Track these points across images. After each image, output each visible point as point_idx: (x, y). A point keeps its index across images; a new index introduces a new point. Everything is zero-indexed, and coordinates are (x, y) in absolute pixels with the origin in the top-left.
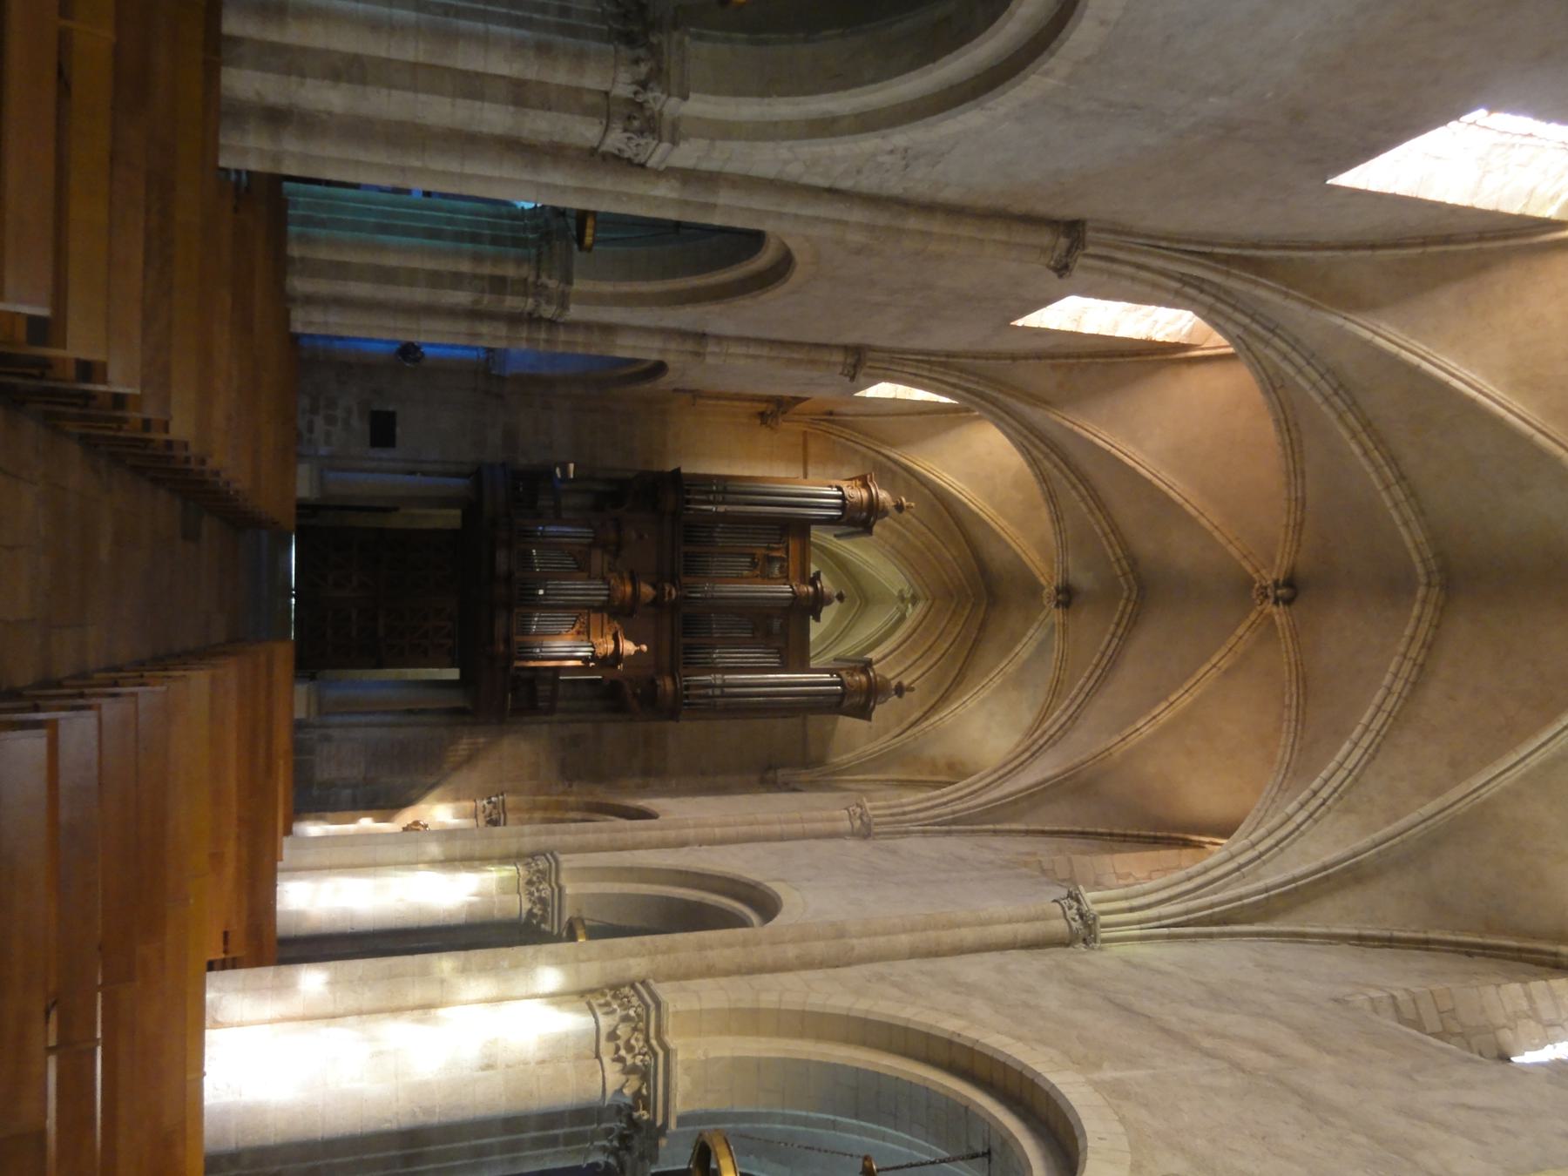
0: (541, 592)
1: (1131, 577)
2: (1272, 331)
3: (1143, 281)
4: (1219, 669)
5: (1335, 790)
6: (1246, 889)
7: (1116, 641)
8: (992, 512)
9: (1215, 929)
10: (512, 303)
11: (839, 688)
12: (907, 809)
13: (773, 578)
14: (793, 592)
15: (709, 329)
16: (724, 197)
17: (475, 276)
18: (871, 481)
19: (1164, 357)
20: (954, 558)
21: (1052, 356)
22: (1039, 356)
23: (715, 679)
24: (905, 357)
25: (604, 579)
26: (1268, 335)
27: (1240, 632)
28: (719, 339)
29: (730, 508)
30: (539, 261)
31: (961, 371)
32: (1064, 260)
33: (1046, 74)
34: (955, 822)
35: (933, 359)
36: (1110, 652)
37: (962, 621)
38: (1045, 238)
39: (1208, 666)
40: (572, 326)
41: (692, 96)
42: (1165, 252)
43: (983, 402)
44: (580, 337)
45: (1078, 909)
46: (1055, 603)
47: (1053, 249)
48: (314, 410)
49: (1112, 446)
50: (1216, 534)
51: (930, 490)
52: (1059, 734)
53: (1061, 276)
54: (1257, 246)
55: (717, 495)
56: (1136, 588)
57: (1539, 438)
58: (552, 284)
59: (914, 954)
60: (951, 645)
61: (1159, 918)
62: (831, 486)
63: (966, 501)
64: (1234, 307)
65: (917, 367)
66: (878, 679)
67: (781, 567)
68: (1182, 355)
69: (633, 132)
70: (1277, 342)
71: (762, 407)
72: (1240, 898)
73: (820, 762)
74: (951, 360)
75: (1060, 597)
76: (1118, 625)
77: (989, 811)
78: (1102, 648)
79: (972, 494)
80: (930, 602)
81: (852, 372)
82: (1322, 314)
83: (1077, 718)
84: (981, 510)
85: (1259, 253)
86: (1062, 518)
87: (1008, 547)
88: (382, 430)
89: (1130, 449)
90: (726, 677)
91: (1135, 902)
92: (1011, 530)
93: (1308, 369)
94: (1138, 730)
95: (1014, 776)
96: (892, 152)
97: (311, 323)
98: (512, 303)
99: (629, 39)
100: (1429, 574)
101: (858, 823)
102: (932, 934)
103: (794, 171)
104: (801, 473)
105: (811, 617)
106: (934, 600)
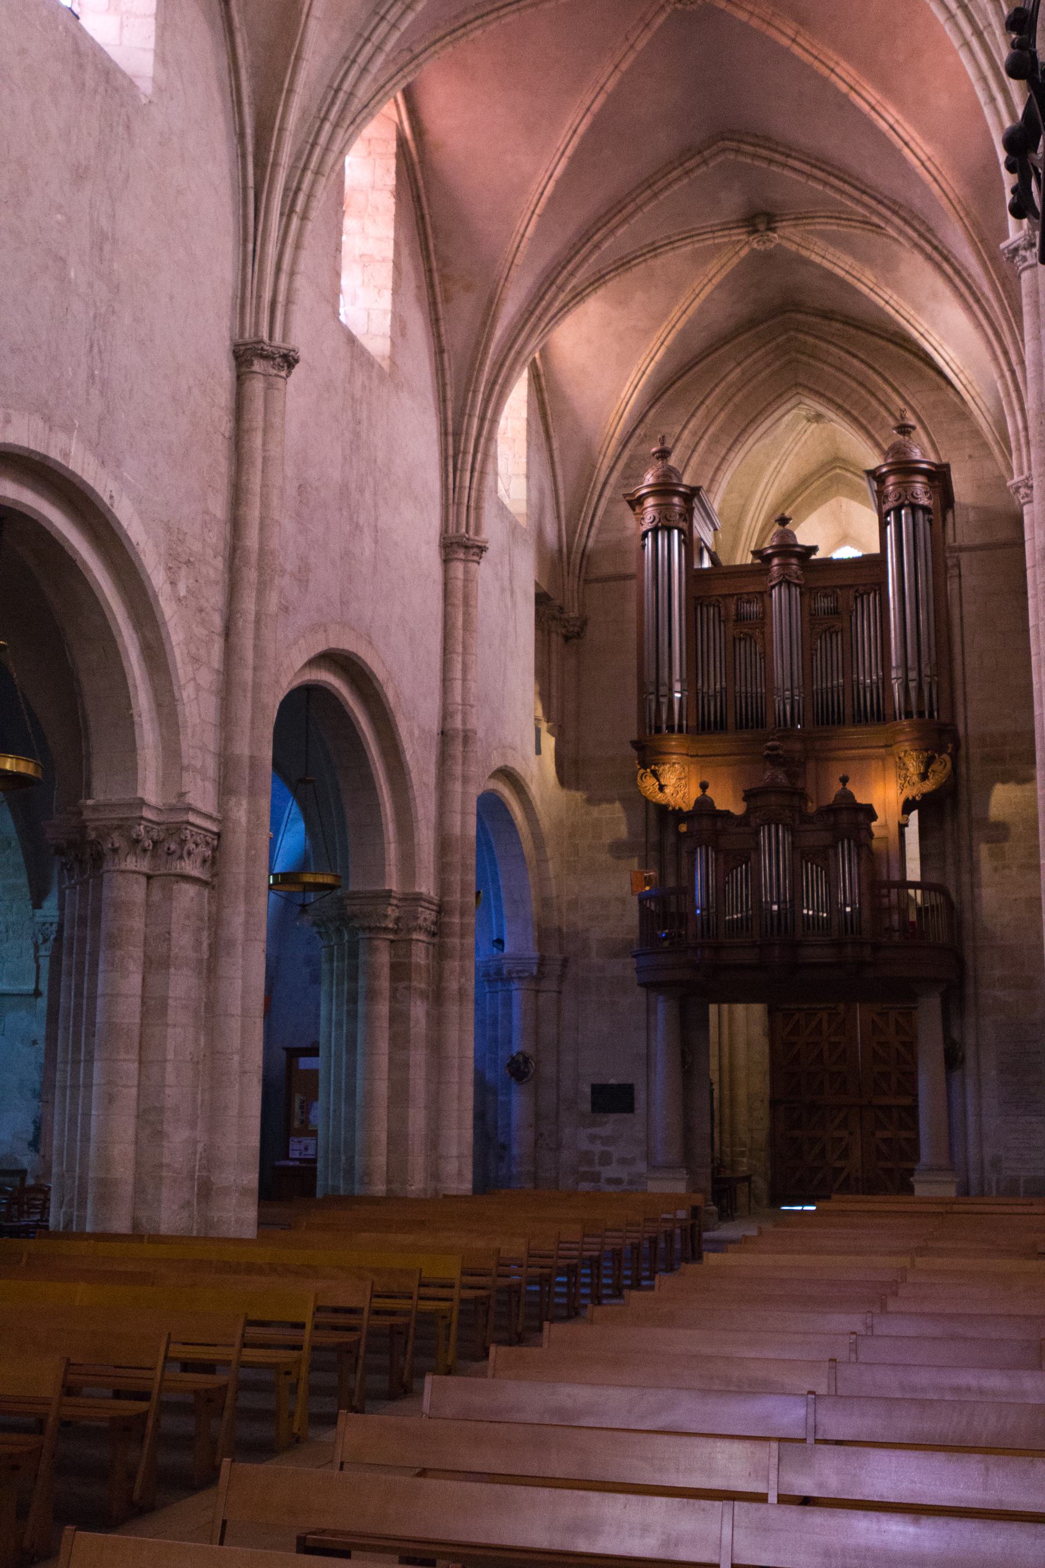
0: (775, 907)
1: (706, 153)
2: (337, 91)
3: (294, 262)
4: (797, 33)
7: (791, 162)
8: (661, 332)
10: (420, 956)
11: (903, 512)
12: (1020, 425)
13: (764, 612)
14: (780, 584)
15: (435, 727)
16: (242, 748)
17: (393, 998)
18: (633, 494)
19: (417, 167)
20: (739, 364)
21: (433, 304)
22: (434, 321)
23: (898, 679)
24: (451, 486)
25: (757, 833)
26: (342, 96)
27: (743, 16)
28: (446, 715)
29: (676, 675)
30: (370, 929)
31: (462, 414)
32: (279, 360)
33: (66, 455)
35: (451, 452)
37: (824, 345)
38: (257, 386)
40: (443, 886)
41: (140, 794)
42: (259, 243)
43: (500, 381)
44: (456, 878)
45: (1025, 249)
46: (771, 234)
48: (595, 1177)
49: (533, 212)
50: (624, 67)
51: (651, 407)
52: (916, 223)
53: (297, 361)
54: (241, 136)
55: (661, 693)
56: (720, 144)
58: (392, 912)
60: (855, 356)
62: (643, 546)
63: (653, 364)
64: (314, 145)
65: (463, 470)
66: (890, 460)
67: (749, 602)
68: (412, 144)
69: (182, 849)
70: (347, 86)
71: (557, 640)
74: (450, 429)
75: (762, 227)
78: (802, 179)
79: (643, 357)
80: (800, 390)
81: (475, 550)
83: (895, 202)
84: (662, 343)
85: (249, 131)
86: (653, 243)
87: (709, 299)
89: (535, 188)
90: (894, 664)
92: (683, 302)
93: (376, 39)
94: (891, 127)
95: (974, 281)
96: (173, 583)
97: (460, 1173)
98: (420, 956)
99: (98, 858)
103: (207, 678)
104: (634, 582)
105: (813, 557)
106: (797, 385)
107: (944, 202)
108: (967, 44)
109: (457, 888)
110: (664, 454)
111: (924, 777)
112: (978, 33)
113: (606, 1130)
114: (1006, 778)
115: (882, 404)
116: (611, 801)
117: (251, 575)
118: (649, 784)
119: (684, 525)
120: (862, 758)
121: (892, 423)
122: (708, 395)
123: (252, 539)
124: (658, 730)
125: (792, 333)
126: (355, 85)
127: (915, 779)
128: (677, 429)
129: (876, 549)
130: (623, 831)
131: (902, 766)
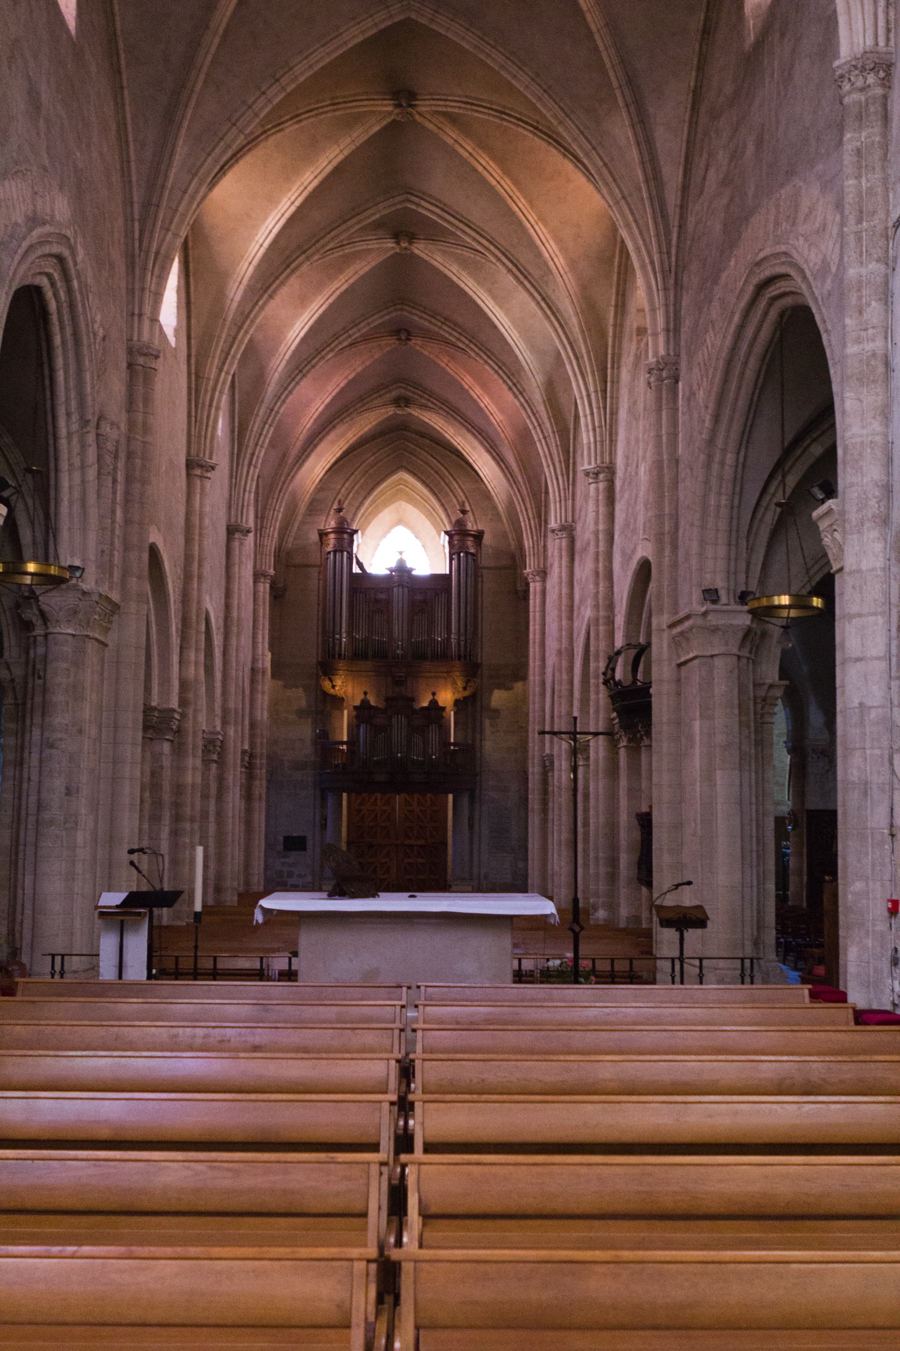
1: (391, 388)
5: (509, 378)
6: (554, 441)
9: (571, 461)
27: (426, 353)
29: (343, 630)
34: (540, 517)
36: (440, 404)
37: (418, 449)
38: (236, 544)
39: (447, 368)
47: (240, 539)
50: (367, 363)
57: (330, 301)
59: (571, 618)
60: (434, 458)
61: (564, 489)
62: (327, 559)
70: (276, 409)
72: (557, 446)
73: (513, 557)
74: (259, 516)
75: (403, 405)
76: (421, 397)
77: (534, 495)
82: (266, 398)
88: (295, 844)
91: (558, 499)
97: (259, 882)
100: (396, 310)
101: (538, 578)
102: (563, 608)
107: (506, 442)
108: (540, 441)
109: (258, 745)
110: (339, 510)
111: (465, 689)
112: (545, 438)
113: (291, 860)
114: (501, 686)
115: (447, 485)
116: (297, 687)
117: (234, 629)
118: (327, 685)
119: (349, 550)
120: (436, 677)
121: (458, 507)
122: (356, 469)
123: (235, 614)
124: (333, 656)
125: (402, 441)
126: (279, 408)
127: (461, 689)
128: (339, 487)
129: (448, 572)
130: (303, 703)
131: (454, 683)
